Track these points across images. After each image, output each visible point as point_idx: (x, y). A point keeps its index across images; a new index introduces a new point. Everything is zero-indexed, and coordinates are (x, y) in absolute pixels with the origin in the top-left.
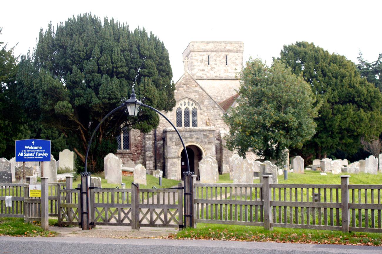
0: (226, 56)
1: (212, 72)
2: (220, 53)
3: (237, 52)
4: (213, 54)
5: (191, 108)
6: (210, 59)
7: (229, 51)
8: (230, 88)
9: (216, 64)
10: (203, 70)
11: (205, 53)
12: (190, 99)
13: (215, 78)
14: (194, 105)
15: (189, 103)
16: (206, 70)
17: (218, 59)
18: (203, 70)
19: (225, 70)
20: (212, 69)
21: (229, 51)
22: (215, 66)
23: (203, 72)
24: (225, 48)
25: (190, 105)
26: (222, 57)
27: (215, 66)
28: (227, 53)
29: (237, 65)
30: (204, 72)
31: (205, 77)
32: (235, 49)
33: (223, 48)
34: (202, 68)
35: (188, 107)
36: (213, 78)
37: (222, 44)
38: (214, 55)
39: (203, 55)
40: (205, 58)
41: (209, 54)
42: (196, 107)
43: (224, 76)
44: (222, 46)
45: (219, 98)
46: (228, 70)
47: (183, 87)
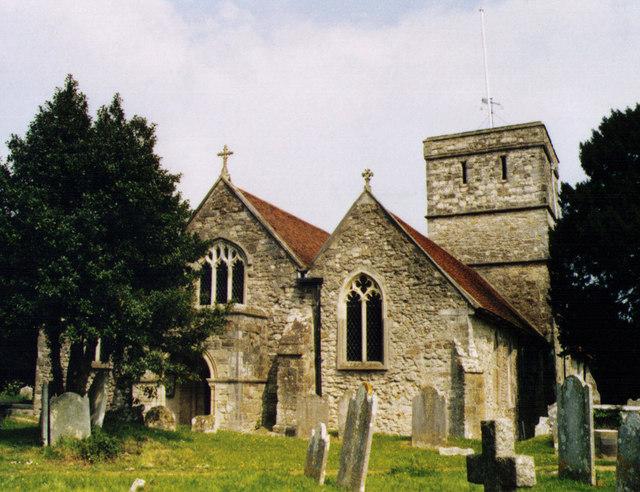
0: (504, 159)
1: (470, 199)
2: (488, 156)
3: (527, 148)
4: (472, 160)
5: (230, 262)
6: (469, 171)
7: (509, 148)
8: (512, 229)
9: (478, 180)
10: (452, 196)
11: (455, 160)
12: (226, 241)
13: (479, 210)
14: (238, 256)
15: (226, 251)
16: (459, 195)
17: (483, 169)
18: (452, 196)
19: (499, 190)
20: (471, 190)
21: (509, 148)
22: (477, 184)
23: (449, 200)
24: (498, 141)
25: (230, 256)
26: (492, 163)
27: (477, 184)
28: (504, 154)
29: (529, 175)
30: (455, 200)
31: (455, 212)
32: (521, 140)
33: (494, 141)
34: (447, 191)
35: (225, 259)
36: (473, 211)
37: (492, 136)
38: (474, 160)
39: (451, 165)
40: (457, 167)
41: (463, 159)
42: (240, 259)
43: (498, 202)
44: (491, 141)
45: (487, 253)
46: (507, 189)
47: (213, 215)
